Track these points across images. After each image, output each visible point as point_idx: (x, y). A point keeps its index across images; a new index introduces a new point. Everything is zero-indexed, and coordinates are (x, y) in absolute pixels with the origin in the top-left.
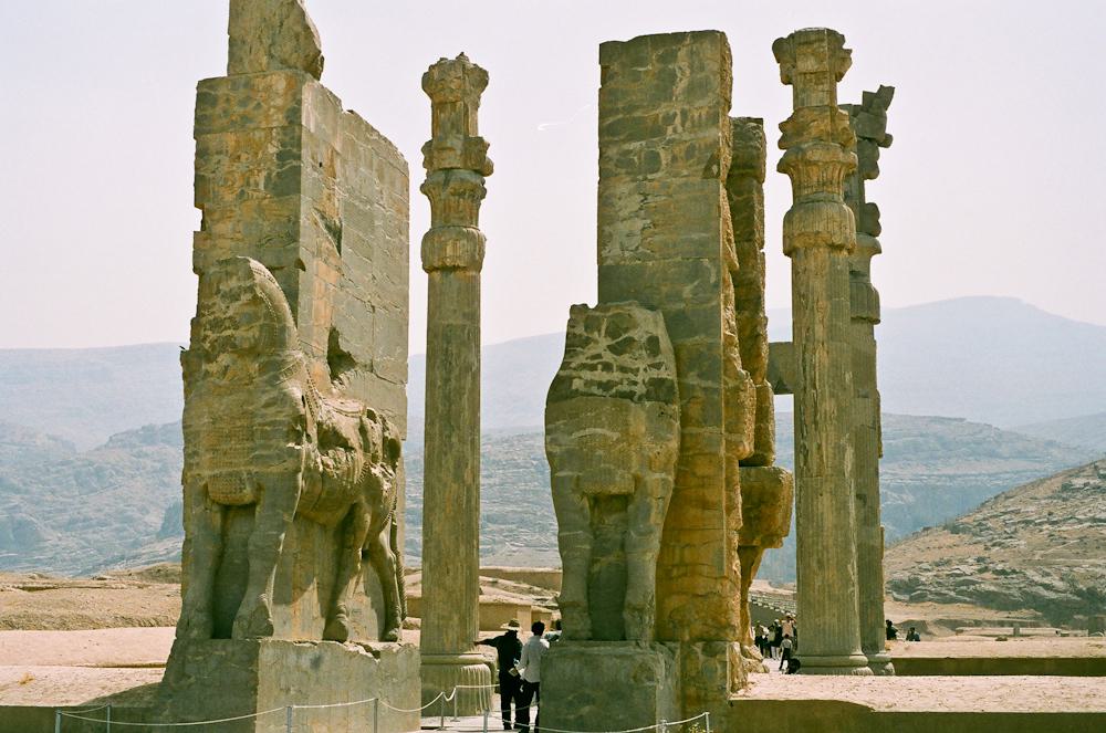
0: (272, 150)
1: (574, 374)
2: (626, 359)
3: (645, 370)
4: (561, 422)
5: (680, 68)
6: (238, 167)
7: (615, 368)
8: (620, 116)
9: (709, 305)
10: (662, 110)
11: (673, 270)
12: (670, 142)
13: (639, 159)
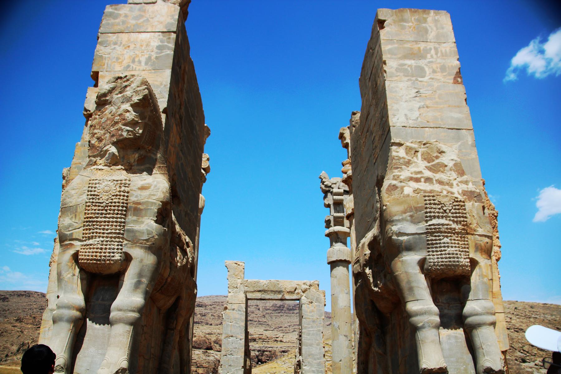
1: (403, 184)
3: (457, 185)
4: (408, 214)
6: (127, 52)
7: (434, 182)
12: (430, 62)
13: (411, 69)
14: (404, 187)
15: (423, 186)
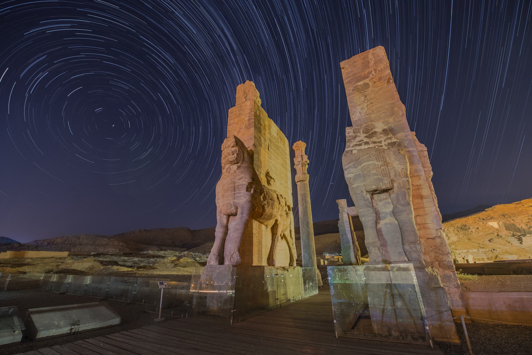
0: (247, 119)
1: (352, 148)
2: (374, 139)
3: (385, 141)
5: (370, 59)
7: (370, 143)
8: (351, 78)
9: (401, 122)
10: (367, 72)
11: (383, 115)
14: (353, 150)
15: (364, 147)
